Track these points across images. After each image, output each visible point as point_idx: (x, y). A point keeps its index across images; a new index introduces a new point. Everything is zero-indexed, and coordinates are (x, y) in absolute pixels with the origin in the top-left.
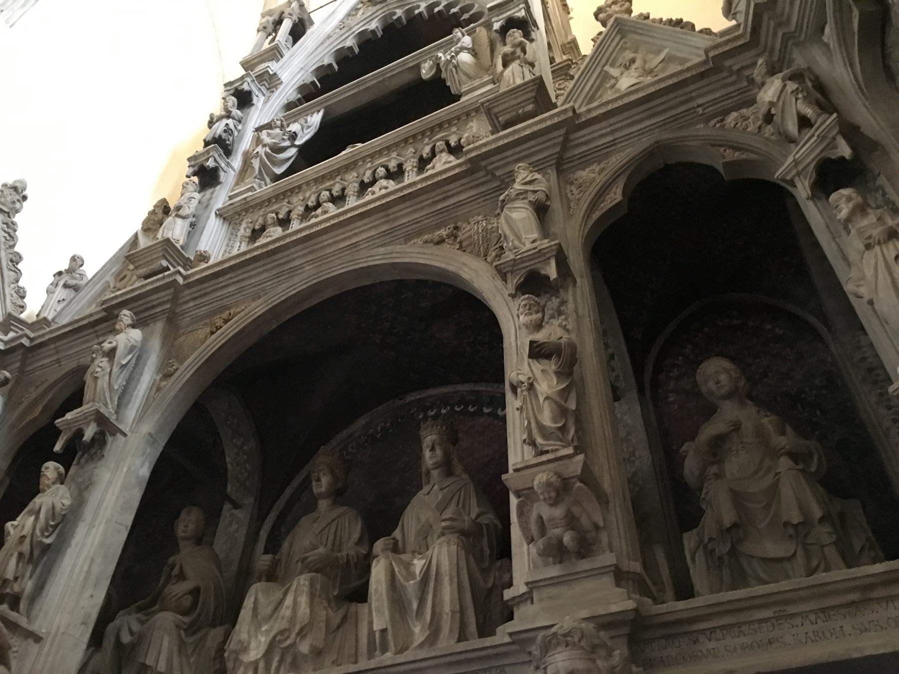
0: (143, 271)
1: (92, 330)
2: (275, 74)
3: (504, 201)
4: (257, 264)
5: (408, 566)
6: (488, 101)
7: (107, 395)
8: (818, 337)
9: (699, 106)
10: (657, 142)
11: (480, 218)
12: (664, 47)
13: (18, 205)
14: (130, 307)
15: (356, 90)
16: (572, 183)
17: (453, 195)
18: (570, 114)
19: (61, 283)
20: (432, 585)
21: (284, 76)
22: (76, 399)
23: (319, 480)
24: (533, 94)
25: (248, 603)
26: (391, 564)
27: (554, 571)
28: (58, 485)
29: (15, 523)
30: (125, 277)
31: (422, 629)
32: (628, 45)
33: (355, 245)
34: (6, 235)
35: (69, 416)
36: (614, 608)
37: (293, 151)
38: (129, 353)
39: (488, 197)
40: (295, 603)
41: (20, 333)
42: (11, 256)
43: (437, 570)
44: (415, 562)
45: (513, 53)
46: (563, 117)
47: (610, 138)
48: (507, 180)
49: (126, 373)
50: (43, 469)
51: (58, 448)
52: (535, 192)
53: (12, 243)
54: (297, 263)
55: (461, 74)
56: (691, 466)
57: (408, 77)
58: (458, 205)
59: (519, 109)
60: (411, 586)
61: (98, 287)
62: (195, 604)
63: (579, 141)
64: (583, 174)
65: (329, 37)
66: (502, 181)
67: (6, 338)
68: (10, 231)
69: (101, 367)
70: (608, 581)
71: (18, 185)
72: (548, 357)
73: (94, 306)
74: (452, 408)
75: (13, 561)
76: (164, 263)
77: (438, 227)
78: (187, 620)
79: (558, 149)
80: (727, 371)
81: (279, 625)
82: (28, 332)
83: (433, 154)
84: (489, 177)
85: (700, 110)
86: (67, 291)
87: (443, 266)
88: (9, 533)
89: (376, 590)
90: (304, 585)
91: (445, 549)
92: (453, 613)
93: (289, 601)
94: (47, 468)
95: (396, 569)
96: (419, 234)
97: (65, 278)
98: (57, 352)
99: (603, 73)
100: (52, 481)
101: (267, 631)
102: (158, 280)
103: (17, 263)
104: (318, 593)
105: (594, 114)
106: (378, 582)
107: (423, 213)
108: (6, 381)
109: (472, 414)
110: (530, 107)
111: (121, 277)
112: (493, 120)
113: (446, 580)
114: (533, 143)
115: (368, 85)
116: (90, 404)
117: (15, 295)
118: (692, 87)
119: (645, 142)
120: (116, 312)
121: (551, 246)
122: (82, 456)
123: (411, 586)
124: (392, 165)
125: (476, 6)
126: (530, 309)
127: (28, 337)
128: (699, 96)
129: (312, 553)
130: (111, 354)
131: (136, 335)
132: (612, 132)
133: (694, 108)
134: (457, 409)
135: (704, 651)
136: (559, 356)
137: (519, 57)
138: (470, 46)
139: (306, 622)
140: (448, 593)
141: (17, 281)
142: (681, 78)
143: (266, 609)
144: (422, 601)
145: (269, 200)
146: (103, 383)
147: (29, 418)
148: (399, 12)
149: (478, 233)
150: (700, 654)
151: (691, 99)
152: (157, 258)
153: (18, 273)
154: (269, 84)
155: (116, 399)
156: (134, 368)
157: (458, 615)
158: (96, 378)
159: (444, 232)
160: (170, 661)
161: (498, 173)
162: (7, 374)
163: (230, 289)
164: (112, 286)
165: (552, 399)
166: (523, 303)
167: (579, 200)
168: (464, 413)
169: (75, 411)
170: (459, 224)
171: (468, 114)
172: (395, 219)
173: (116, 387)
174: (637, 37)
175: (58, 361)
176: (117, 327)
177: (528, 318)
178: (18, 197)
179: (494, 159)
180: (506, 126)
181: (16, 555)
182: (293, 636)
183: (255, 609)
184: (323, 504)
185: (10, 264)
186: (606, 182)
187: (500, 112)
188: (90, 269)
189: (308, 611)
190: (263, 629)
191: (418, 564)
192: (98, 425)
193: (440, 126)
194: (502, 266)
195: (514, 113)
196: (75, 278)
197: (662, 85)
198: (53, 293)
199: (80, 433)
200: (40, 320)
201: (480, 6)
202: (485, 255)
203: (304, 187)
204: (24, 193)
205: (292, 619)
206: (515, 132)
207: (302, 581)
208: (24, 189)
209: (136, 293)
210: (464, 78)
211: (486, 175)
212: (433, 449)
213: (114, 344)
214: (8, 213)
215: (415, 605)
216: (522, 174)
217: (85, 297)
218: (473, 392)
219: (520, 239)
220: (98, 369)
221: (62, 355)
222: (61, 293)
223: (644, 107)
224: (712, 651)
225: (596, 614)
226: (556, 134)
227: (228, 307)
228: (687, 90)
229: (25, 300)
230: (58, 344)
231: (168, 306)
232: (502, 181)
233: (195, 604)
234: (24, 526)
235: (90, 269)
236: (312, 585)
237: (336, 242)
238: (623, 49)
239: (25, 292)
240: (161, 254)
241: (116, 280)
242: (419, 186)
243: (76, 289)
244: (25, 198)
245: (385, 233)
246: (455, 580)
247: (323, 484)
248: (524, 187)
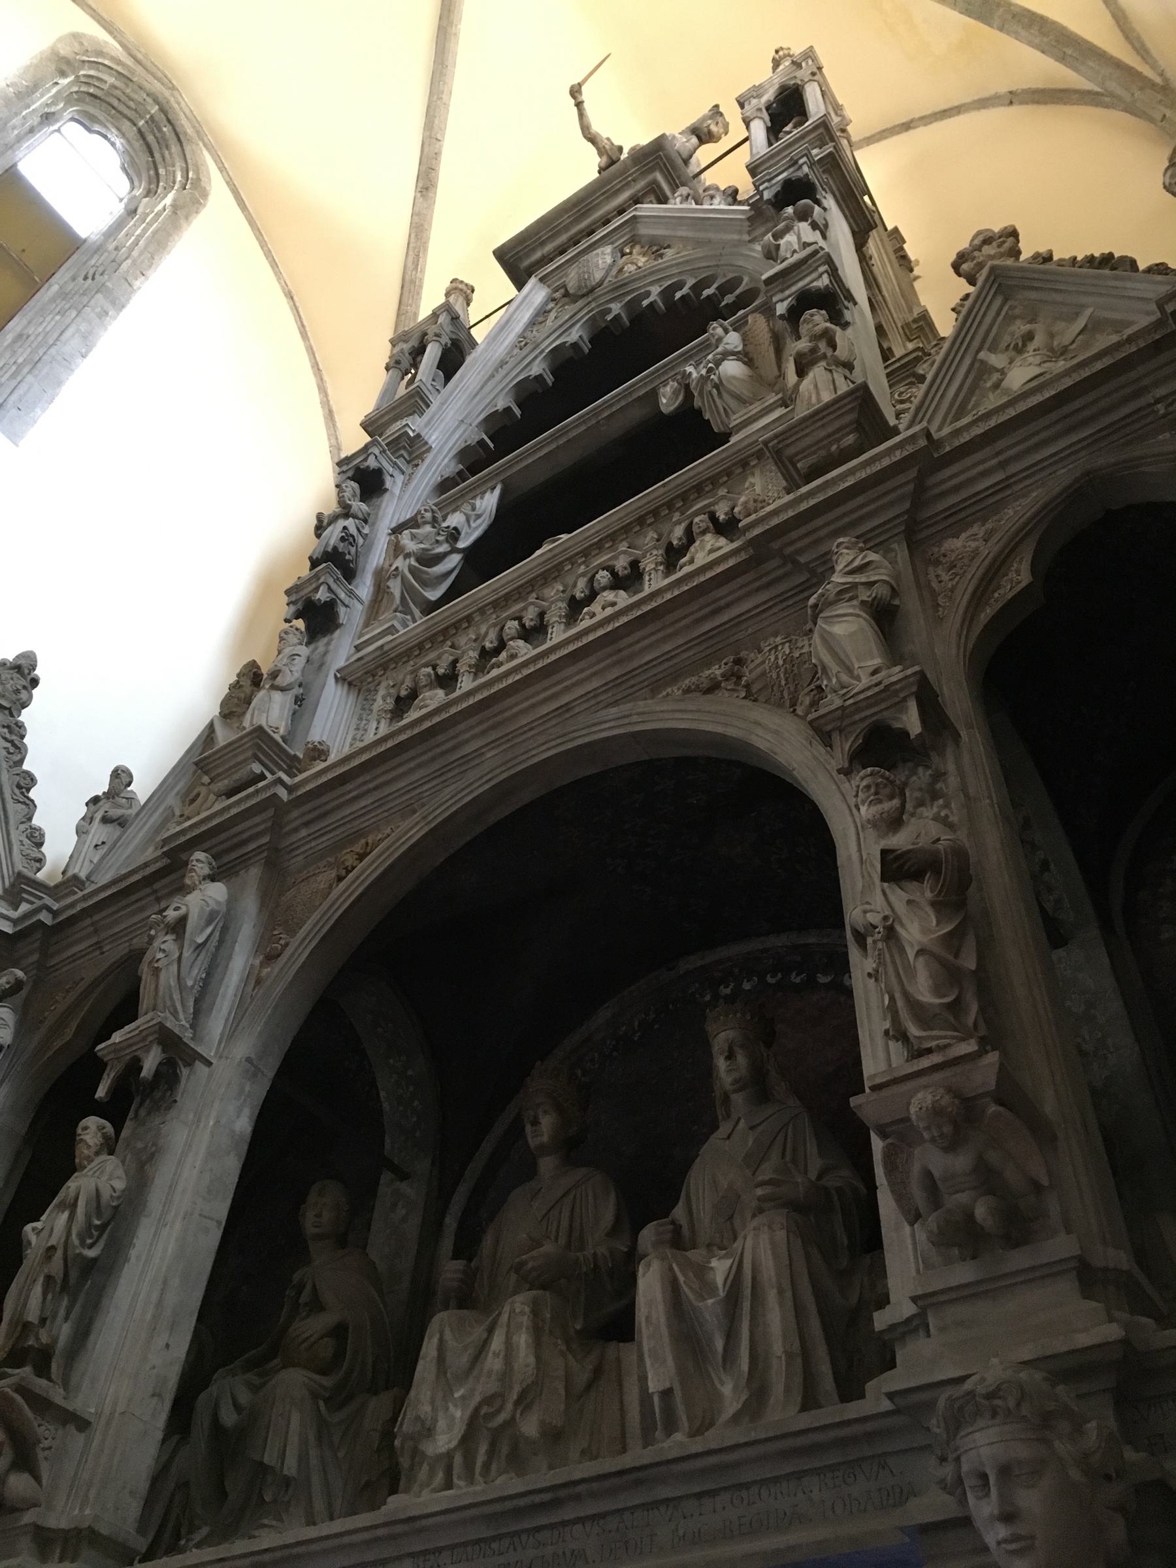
0: (223, 784)
1: (148, 890)
2: (418, 436)
3: (816, 606)
4: (406, 756)
5: (701, 1271)
6: (776, 436)
7: (177, 996)
9: (1157, 401)
10: (1088, 473)
11: (779, 640)
12: (1083, 306)
13: (24, 695)
14: (207, 845)
15: (553, 446)
16: (937, 563)
17: (728, 606)
18: (922, 442)
19: (99, 816)
20: (746, 1305)
21: (433, 438)
22: (126, 1009)
23: (535, 1122)
24: (853, 416)
25: (429, 1348)
26: (671, 1269)
27: (963, 1273)
28: (104, 1157)
29: (38, 1225)
30: (198, 795)
31: (735, 1388)
32: (1017, 311)
33: (567, 707)
34: (8, 745)
35: (117, 1037)
37: (455, 560)
38: (208, 923)
39: (791, 602)
40: (509, 1345)
41: (38, 903)
42: (18, 778)
43: (754, 1279)
44: (714, 1263)
45: (814, 350)
46: (909, 449)
47: (1000, 476)
48: (820, 570)
49: (204, 958)
50: (79, 1131)
51: (101, 1092)
52: (870, 585)
53: (17, 758)
54: (468, 749)
55: (725, 395)
57: (638, 414)
58: (737, 622)
59: (831, 444)
60: (710, 1308)
61: (156, 817)
62: (339, 1355)
63: (944, 487)
64: (955, 545)
65: (502, 363)
66: (812, 572)
67: (15, 915)
68: (14, 737)
69: (164, 951)
70: (1067, 1286)
71: (22, 662)
72: (917, 876)
73: (151, 849)
75: (38, 1289)
76: (257, 768)
78: (327, 1381)
79: (907, 505)
81: (485, 1386)
82: (48, 901)
83: (690, 537)
84: (789, 566)
85: (1161, 408)
86: (109, 828)
87: (720, 729)
88: (29, 1243)
89: (648, 1318)
90: (522, 1313)
91: (764, 1238)
92: (789, 1355)
93: (497, 1343)
94: (86, 1128)
95: (681, 1279)
96: (674, 677)
97: (105, 806)
98: (96, 931)
99: (977, 365)
100: (94, 1150)
101: (463, 1397)
102: (248, 797)
103: (28, 790)
104: (547, 1328)
105: (966, 437)
108: (18, 985)
110: (850, 439)
111: (190, 798)
112: (785, 466)
113: (772, 1297)
114: (860, 500)
115: (571, 435)
116: (148, 1017)
117: (26, 841)
118: (1141, 370)
119: (1064, 476)
120: (184, 857)
121: (906, 677)
122: (141, 1104)
123: (710, 1308)
124: (621, 564)
125: (746, 279)
126: (876, 793)
127: (49, 909)
128: (1156, 384)
129: (534, 1253)
130: (178, 928)
131: (217, 892)
132: (1002, 465)
133: (1150, 405)
134: (770, 980)
136: (937, 873)
137: (824, 357)
138: (740, 348)
139: (529, 1381)
140: (776, 1318)
141: (30, 819)
142: (1120, 355)
143: (459, 1360)
144: (731, 1336)
145: (420, 646)
146: (168, 977)
147: (58, 1044)
148: (616, 308)
149: (777, 667)
151: (1144, 390)
152: (245, 760)
153: (31, 805)
154: (410, 454)
155: (191, 1004)
156: (218, 948)
157: (799, 1361)
158: (157, 971)
159: (717, 671)
160: (303, 1458)
161: (802, 560)
162: (20, 974)
164: (178, 813)
165: (932, 954)
166: (864, 783)
167: (952, 590)
169: (127, 1028)
170: (743, 654)
171: (744, 464)
172: (631, 657)
173: (190, 983)
174: (1033, 295)
175: (98, 946)
176: (188, 881)
177: (875, 809)
178: (23, 682)
179: (794, 535)
180: (808, 479)
181: (41, 1279)
182: (509, 1406)
183: (441, 1359)
184: (547, 1165)
185: (17, 791)
186: (1001, 552)
187: (797, 454)
188: (142, 788)
189: (532, 1360)
190: (456, 1395)
191: (720, 1268)
192: (164, 1051)
193: (699, 489)
194: (822, 721)
195: (823, 453)
196: (120, 806)
197: (1086, 373)
198: (86, 833)
199: (135, 1065)
200: (68, 880)
201: (752, 279)
202: (793, 704)
203: (477, 618)
204: (32, 675)
205: (506, 1376)
206: (826, 484)
207: (518, 1307)
208: (33, 667)
209: (214, 822)
210: (733, 403)
211: (784, 565)
212: (730, 1056)
213: (183, 910)
214: (9, 709)
215: (719, 1344)
216: (846, 556)
217: (137, 834)
219: (849, 670)
220: (160, 955)
221: (104, 935)
222: (99, 832)
223: (1054, 416)
226: (901, 479)
227: (360, 834)
228: (1133, 375)
229: (43, 849)
230: (96, 917)
231: (265, 839)
232: (812, 572)
233: (339, 1355)
234: (52, 1229)
235: (142, 788)
236: (535, 1313)
237: (533, 706)
238: (1010, 319)
239: (42, 835)
240: (250, 753)
241: (183, 802)
242: (669, 596)
243: (122, 822)
244: (35, 682)
245: (617, 683)
246: (789, 1294)
247: (544, 1128)
248: (849, 579)
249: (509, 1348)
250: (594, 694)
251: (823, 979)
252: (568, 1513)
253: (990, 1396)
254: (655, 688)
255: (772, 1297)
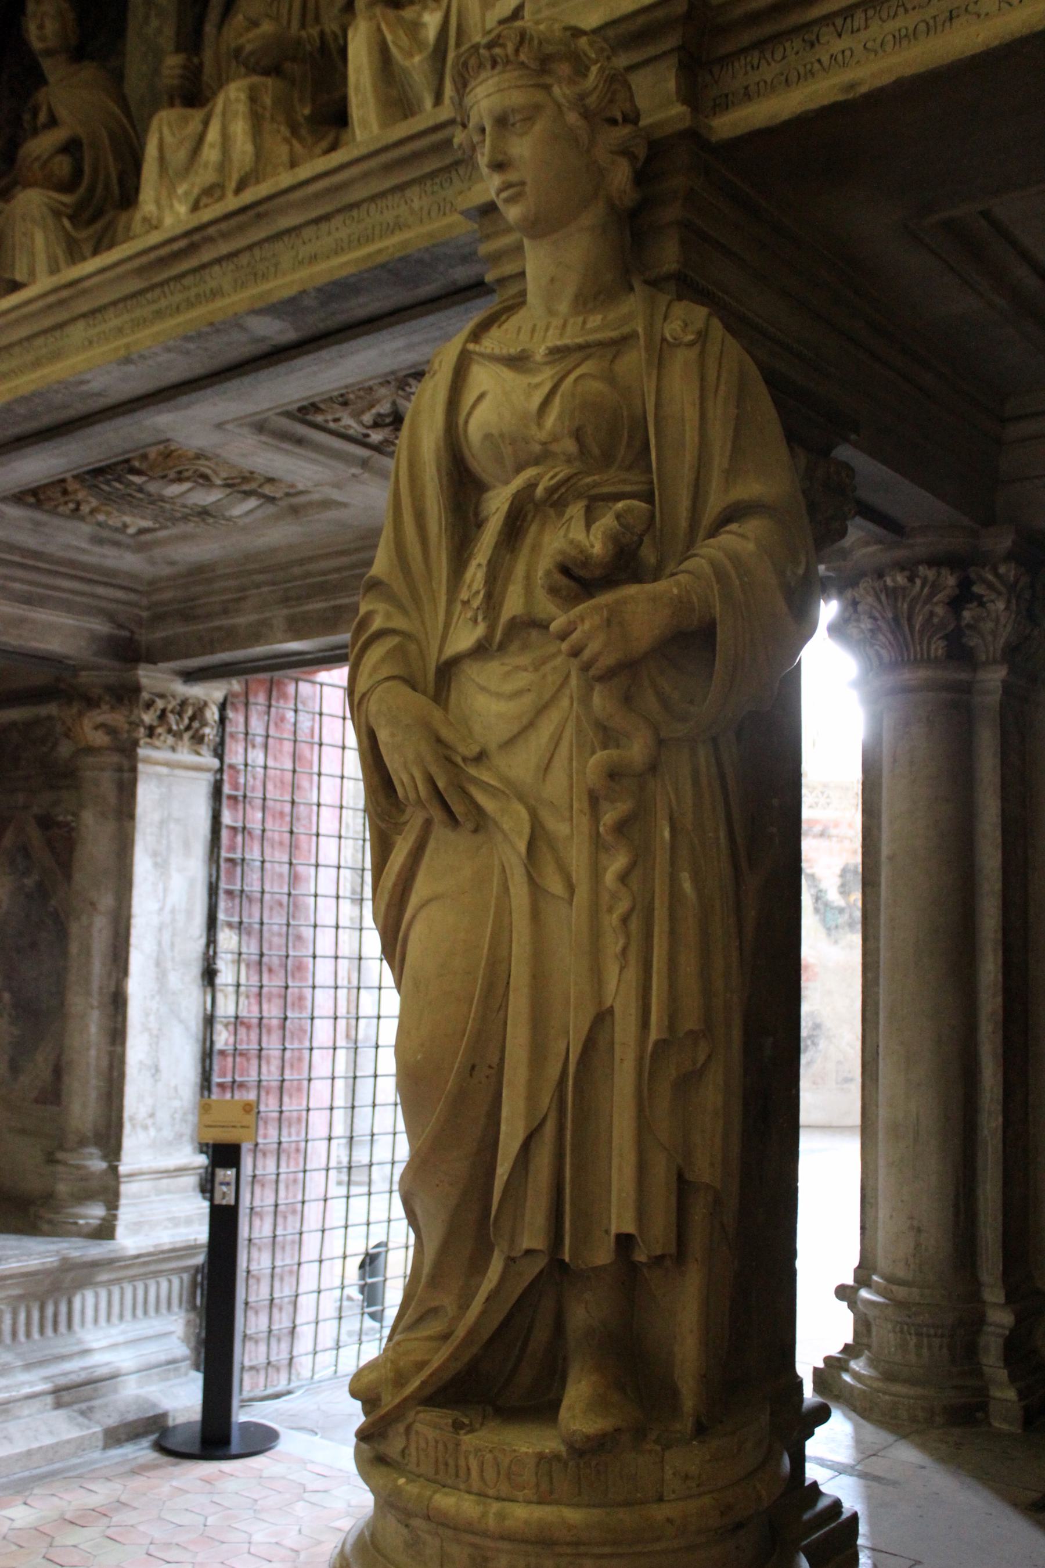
5: (414, 28)
25: (151, 151)
26: (379, 29)
40: (225, 137)
43: (459, 26)
62: (78, 172)
78: (67, 199)
81: (204, 177)
90: (238, 100)
93: (213, 135)
95: (389, 38)
104: (268, 115)
129: (251, 35)
135: (825, 59)
139: (248, 169)
143: (179, 157)
150: (817, 66)
183: (162, 159)
189: (249, 148)
190: (180, 191)
191: (432, 20)
207: (234, 94)
224: (840, 58)
225: (618, 14)
233: (78, 172)
236: (253, 99)
249: (225, 137)
252: (207, 255)
253: (490, 46)
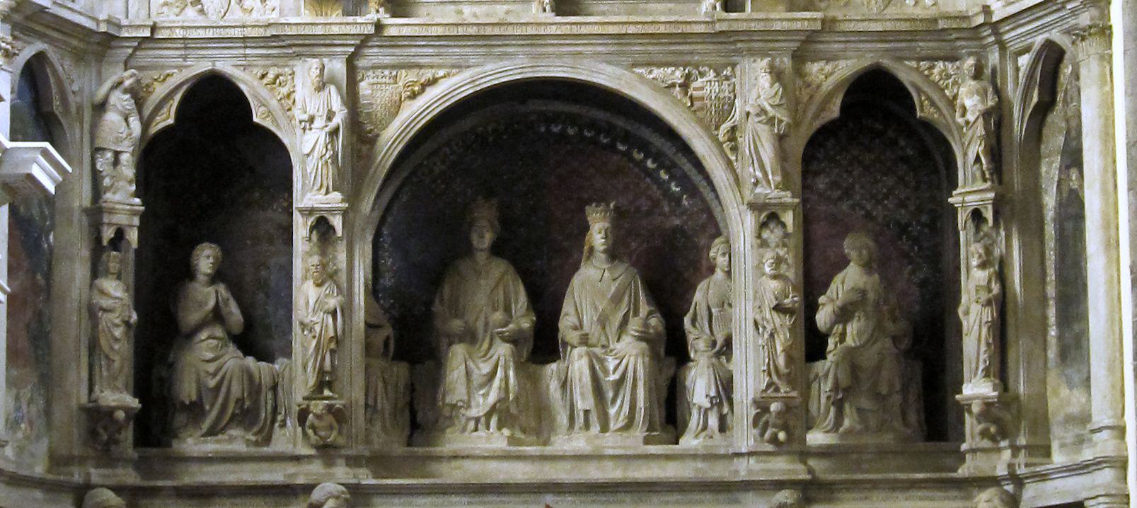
8: (936, 171)
23: (482, 237)
27: (770, 448)
36: (800, 477)
56: (823, 317)
74: (581, 130)
77: (668, 65)
80: (868, 248)
96: (648, 64)
106: (581, 373)
107: (657, 48)
109: (605, 147)
113: (641, 384)
134: (587, 134)
163: (425, 50)
168: (594, 141)
175: (185, 58)
184: (481, 257)
215: (610, 395)
218: (608, 123)
242: (663, 29)
247: (484, 238)
250: (600, 53)
251: (621, 148)
254: (635, 65)
255: (641, 384)
